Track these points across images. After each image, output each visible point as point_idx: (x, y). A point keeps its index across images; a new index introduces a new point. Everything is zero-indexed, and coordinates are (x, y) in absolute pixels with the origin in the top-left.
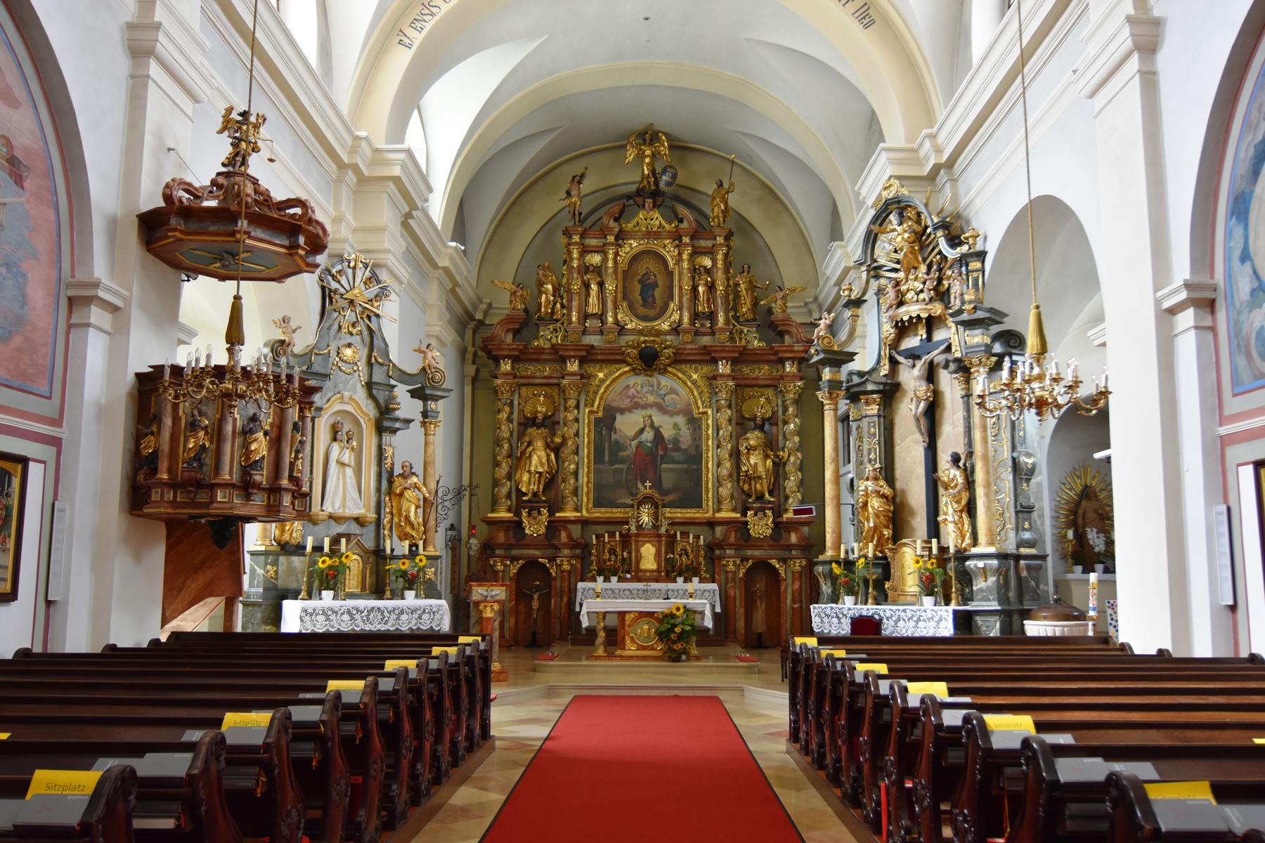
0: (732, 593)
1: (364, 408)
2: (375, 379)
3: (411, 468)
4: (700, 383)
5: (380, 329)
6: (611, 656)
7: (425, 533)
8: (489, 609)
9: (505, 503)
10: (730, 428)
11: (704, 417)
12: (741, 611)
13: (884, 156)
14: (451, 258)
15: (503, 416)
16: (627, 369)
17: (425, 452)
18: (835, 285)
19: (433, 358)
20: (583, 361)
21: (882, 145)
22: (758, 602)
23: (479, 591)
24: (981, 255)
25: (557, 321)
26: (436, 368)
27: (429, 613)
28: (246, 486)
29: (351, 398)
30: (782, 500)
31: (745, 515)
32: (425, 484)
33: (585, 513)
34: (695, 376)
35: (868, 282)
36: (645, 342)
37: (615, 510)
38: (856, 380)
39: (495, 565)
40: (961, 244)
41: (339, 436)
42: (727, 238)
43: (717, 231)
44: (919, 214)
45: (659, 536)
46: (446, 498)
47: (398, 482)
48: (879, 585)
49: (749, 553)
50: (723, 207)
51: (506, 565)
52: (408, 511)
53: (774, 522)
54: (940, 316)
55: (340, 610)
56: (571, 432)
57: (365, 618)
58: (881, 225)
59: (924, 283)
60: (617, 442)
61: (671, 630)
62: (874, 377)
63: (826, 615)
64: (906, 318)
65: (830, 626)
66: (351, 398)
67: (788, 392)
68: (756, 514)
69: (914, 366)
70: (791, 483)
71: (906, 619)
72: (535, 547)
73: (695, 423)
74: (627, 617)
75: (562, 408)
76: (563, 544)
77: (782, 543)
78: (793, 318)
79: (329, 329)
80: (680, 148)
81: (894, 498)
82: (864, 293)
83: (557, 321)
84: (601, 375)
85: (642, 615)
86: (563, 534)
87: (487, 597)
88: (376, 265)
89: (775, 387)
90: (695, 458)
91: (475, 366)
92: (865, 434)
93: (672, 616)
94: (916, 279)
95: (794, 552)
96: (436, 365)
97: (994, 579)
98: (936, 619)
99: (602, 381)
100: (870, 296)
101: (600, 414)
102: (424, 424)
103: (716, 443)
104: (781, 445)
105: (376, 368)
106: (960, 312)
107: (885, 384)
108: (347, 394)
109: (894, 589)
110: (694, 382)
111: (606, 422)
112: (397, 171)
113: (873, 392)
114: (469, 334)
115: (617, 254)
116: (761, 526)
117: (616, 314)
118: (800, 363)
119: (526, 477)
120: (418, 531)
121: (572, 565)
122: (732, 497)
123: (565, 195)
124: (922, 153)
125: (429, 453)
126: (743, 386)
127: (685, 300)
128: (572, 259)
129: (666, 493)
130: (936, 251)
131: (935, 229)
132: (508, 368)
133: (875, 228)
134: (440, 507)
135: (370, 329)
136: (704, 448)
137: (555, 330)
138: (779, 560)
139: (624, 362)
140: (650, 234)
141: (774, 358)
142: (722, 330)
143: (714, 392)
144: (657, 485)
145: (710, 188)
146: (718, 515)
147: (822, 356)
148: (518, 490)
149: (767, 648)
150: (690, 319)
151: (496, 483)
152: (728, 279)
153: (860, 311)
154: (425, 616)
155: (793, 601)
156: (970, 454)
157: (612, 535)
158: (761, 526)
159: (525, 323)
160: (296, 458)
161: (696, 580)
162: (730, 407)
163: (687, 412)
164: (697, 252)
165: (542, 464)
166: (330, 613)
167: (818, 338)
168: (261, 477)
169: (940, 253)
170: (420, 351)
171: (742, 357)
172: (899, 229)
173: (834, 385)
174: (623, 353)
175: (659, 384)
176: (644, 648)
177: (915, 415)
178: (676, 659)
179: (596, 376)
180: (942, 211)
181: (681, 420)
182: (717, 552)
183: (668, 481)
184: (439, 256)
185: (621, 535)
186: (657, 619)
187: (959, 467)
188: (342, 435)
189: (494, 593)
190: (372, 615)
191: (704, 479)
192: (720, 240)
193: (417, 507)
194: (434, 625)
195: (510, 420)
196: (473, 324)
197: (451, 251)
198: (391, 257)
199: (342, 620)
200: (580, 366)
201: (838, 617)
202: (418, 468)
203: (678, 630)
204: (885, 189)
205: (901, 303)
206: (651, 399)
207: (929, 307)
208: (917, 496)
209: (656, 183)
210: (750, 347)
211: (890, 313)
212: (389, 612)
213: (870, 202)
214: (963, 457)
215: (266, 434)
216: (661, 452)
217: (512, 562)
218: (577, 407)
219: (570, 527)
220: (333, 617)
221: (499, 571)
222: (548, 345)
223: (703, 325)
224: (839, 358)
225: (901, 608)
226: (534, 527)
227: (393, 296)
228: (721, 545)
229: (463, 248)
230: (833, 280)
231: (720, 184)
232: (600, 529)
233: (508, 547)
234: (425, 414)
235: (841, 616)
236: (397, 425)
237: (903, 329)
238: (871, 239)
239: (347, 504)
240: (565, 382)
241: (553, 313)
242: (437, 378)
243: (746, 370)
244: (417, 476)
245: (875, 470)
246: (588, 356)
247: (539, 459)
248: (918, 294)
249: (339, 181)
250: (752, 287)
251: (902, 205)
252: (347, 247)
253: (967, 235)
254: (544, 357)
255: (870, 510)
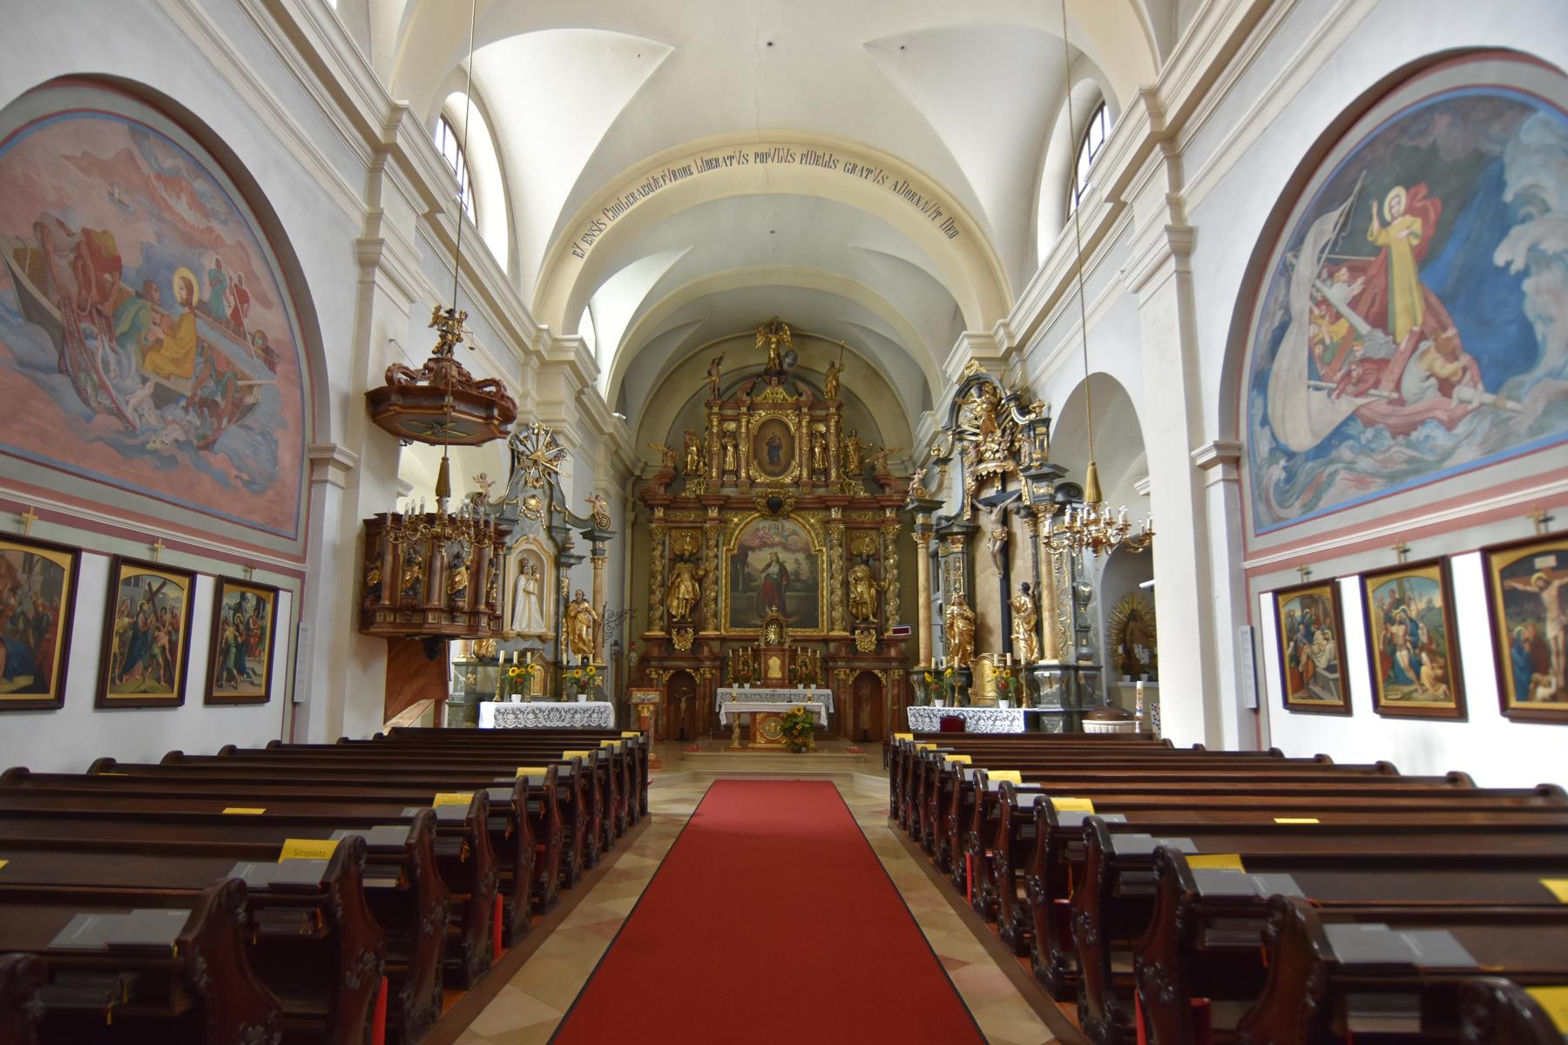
0: (843, 697)
2: (553, 524)
4: (817, 526)
5: (558, 483)
6: (744, 748)
7: (594, 648)
9: (658, 624)
10: (841, 563)
11: (820, 554)
12: (850, 712)
13: (966, 342)
14: (615, 426)
15: (657, 553)
16: (757, 515)
17: (595, 583)
18: (927, 446)
20: (721, 509)
21: (964, 332)
22: (864, 704)
24: (1046, 422)
25: (701, 476)
28: (452, 611)
29: (535, 539)
30: (884, 621)
31: (853, 633)
32: (594, 609)
33: (723, 631)
34: (812, 521)
35: (953, 444)
36: (771, 493)
37: (747, 629)
38: (944, 523)
39: (650, 674)
40: (1029, 412)
41: (525, 571)
42: (839, 408)
43: (830, 403)
44: (995, 388)
45: (784, 650)
47: (573, 607)
48: (963, 691)
49: (857, 664)
50: (834, 383)
51: (659, 674)
52: (581, 630)
53: (877, 639)
54: (1012, 472)
56: (712, 566)
58: (964, 397)
59: (999, 445)
60: (749, 574)
61: (794, 727)
62: (959, 521)
64: (984, 473)
66: (535, 539)
67: (888, 533)
68: (862, 633)
69: (991, 512)
70: (891, 607)
72: (683, 659)
73: (812, 559)
74: (758, 716)
75: (704, 547)
76: (706, 657)
77: (884, 656)
78: (893, 473)
79: (518, 483)
80: (799, 335)
81: (975, 620)
82: (950, 453)
83: (701, 476)
84: (736, 520)
85: (770, 715)
86: (706, 649)
88: (555, 432)
89: (878, 529)
90: (813, 587)
92: (952, 567)
93: (794, 715)
94: (993, 441)
95: (893, 664)
97: (1058, 686)
99: (737, 525)
100: (955, 455)
101: (735, 552)
102: (593, 560)
103: (829, 575)
104: (882, 577)
105: (555, 515)
106: (1029, 468)
107: (967, 527)
108: (531, 536)
109: (976, 694)
110: (812, 526)
111: (740, 559)
112: (572, 356)
113: (958, 533)
114: (629, 487)
115: (748, 422)
116: (866, 643)
117: (748, 473)
118: (898, 510)
119: (675, 603)
120: (588, 646)
121: (713, 674)
122: (843, 619)
123: (706, 374)
124: (997, 339)
126: (852, 529)
127: (804, 459)
128: (712, 426)
129: (790, 615)
130: (1009, 418)
131: (1009, 400)
132: (661, 514)
133: (959, 400)
136: (820, 579)
137: (699, 484)
138: (881, 670)
139: (755, 509)
140: (775, 406)
141: (877, 505)
142: (835, 483)
143: (827, 534)
144: (782, 609)
145: (824, 368)
146: (831, 634)
147: (916, 504)
148: (669, 614)
149: (871, 741)
150: (808, 474)
151: (651, 608)
152: (839, 442)
153: (947, 468)
154: (595, 715)
155: (893, 704)
156: (1038, 584)
157: (745, 649)
158: (866, 643)
159: (675, 478)
160: (492, 588)
161: (813, 686)
162: (841, 545)
163: (806, 550)
164: (814, 420)
165: (688, 592)
167: (913, 489)
168: (463, 603)
169: (1012, 420)
170: (590, 501)
171: (850, 505)
172: (978, 400)
173: (926, 528)
174: (754, 502)
175: (783, 527)
176: (772, 742)
177: (993, 552)
178: (798, 751)
179: (732, 521)
180: (1014, 385)
181: (801, 556)
182: (831, 664)
183: (790, 606)
185: (752, 649)
186: (782, 718)
187: (1028, 595)
188: (528, 569)
189: (650, 697)
191: (820, 604)
192: (832, 410)
193: (588, 627)
195: (662, 556)
197: (615, 420)
200: (719, 512)
202: (589, 596)
203: (799, 727)
204: (967, 368)
205: (980, 461)
206: (777, 539)
207: (1003, 464)
208: (994, 618)
209: (781, 364)
210: (857, 497)
211: (972, 469)
213: (955, 379)
214: (1032, 586)
215: (467, 568)
216: (785, 583)
217: (664, 671)
218: (717, 546)
219: (712, 643)
221: (653, 679)
222: (693, 496)
223: (819, 479)
225: (982, 709)
226: (682, 643)
227: (569, 457)
228: (834, 658)
230: (925, 443)
231: (833, 365)
232: (734, 645)
233: (661, 659)
234: (594, 552)
236: (572, 561)
237: (982, 482)
238: (956, 409)
239: (532, 624)
240: (707, 525)
241: (697, 470)
243: (854, 515)
245: (959, 597)
246: (726, 505)
247: (686, 588)
248: (994, 453)
249: (525, 364)
250: (858, 448)
251: (981, 381)
253: (1035, 405)
254: (690, 505)
255: (956, 629)
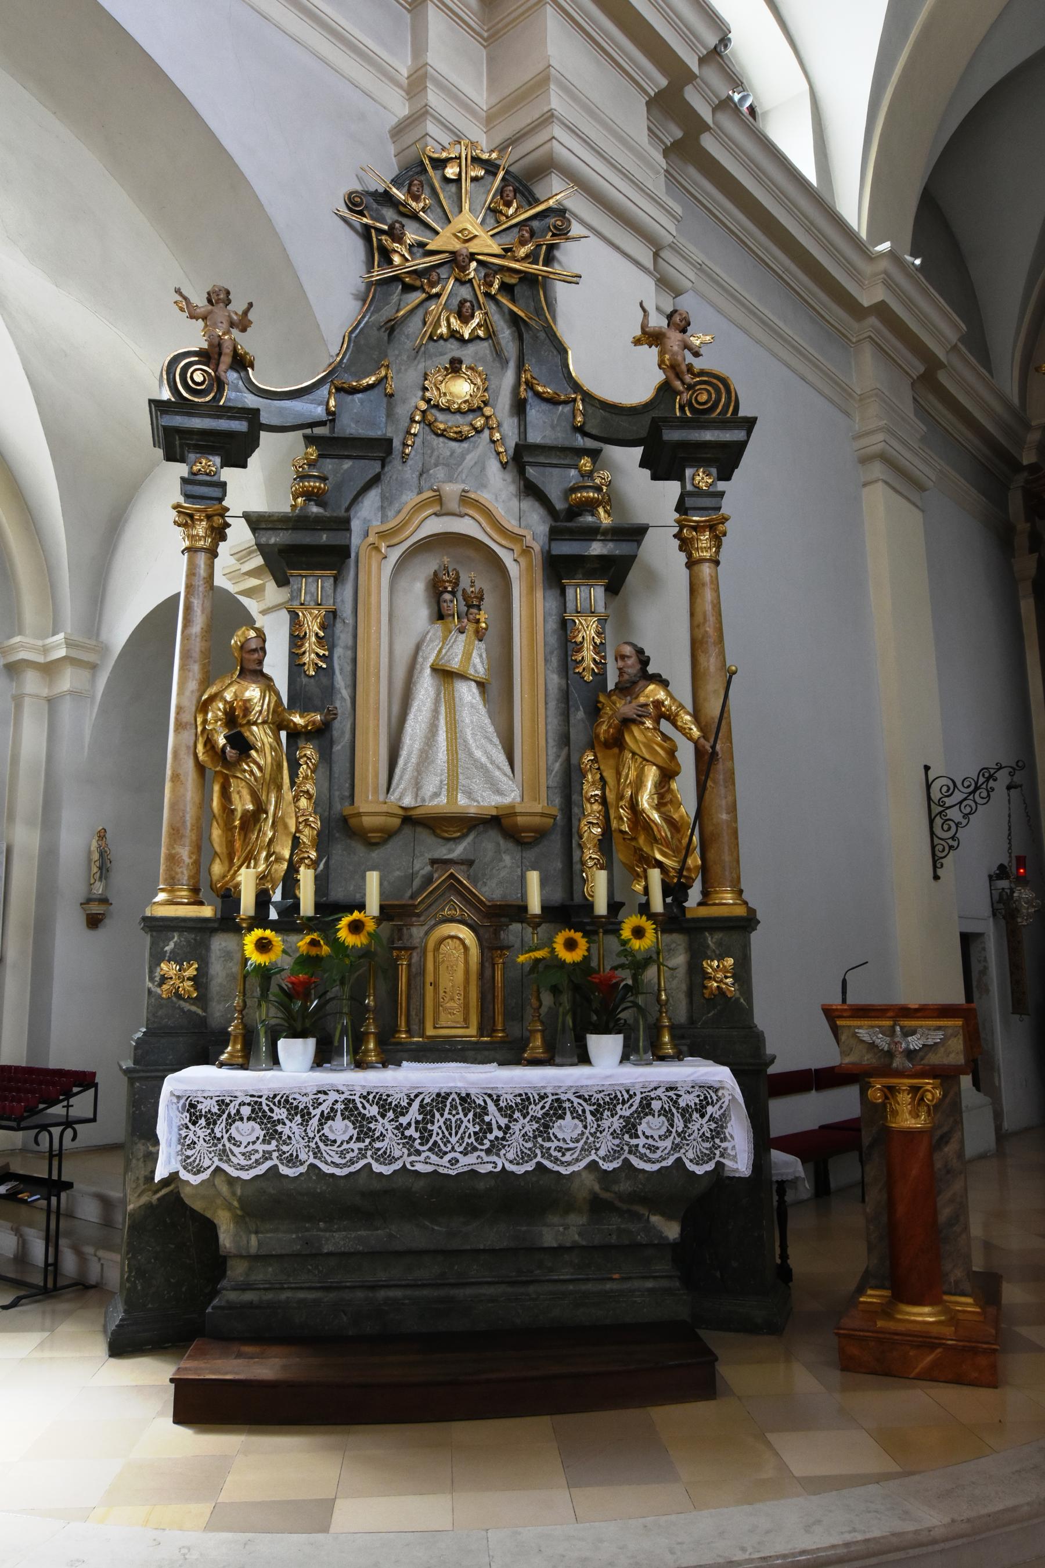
1: (511, 524)
2: (535, 437)
3: (645, 662)
8: (904, 1098)
14: (889, 283)
17: (692, 614)
19: (687, 346)
23: (864, 1034)
26: (702, 373)
27: (664, 1112)
32: (696, 716)
46: (949, 802)
52: (638, 784)
55: (317, 1104)
57: (411, 1132)
66: (465, 499)
87: (890, 1054)
91: (1035, 556)
96: (698, 364)
105: (535, 412)
108: (451, 489)
114: (1016, 502)
125: (699, 618)
134: (938, 821)
135: (515, 321)
154: (652, 1125)
166: (280, 1113)
184: (860, 284)
188: (454, 604)
189: (915, 1042)
190: (439, 1120)
194: (688, 1155)
196: (1021, 479)
197: (884, 264)
198: (557, 131)
199: (325, 1140)
212: (507, 1111)
220: (291, 1128)
229: (918, 262)
239: (462, 780)
242: (704, 397)
244: (664, 683)
252: (431, 128)
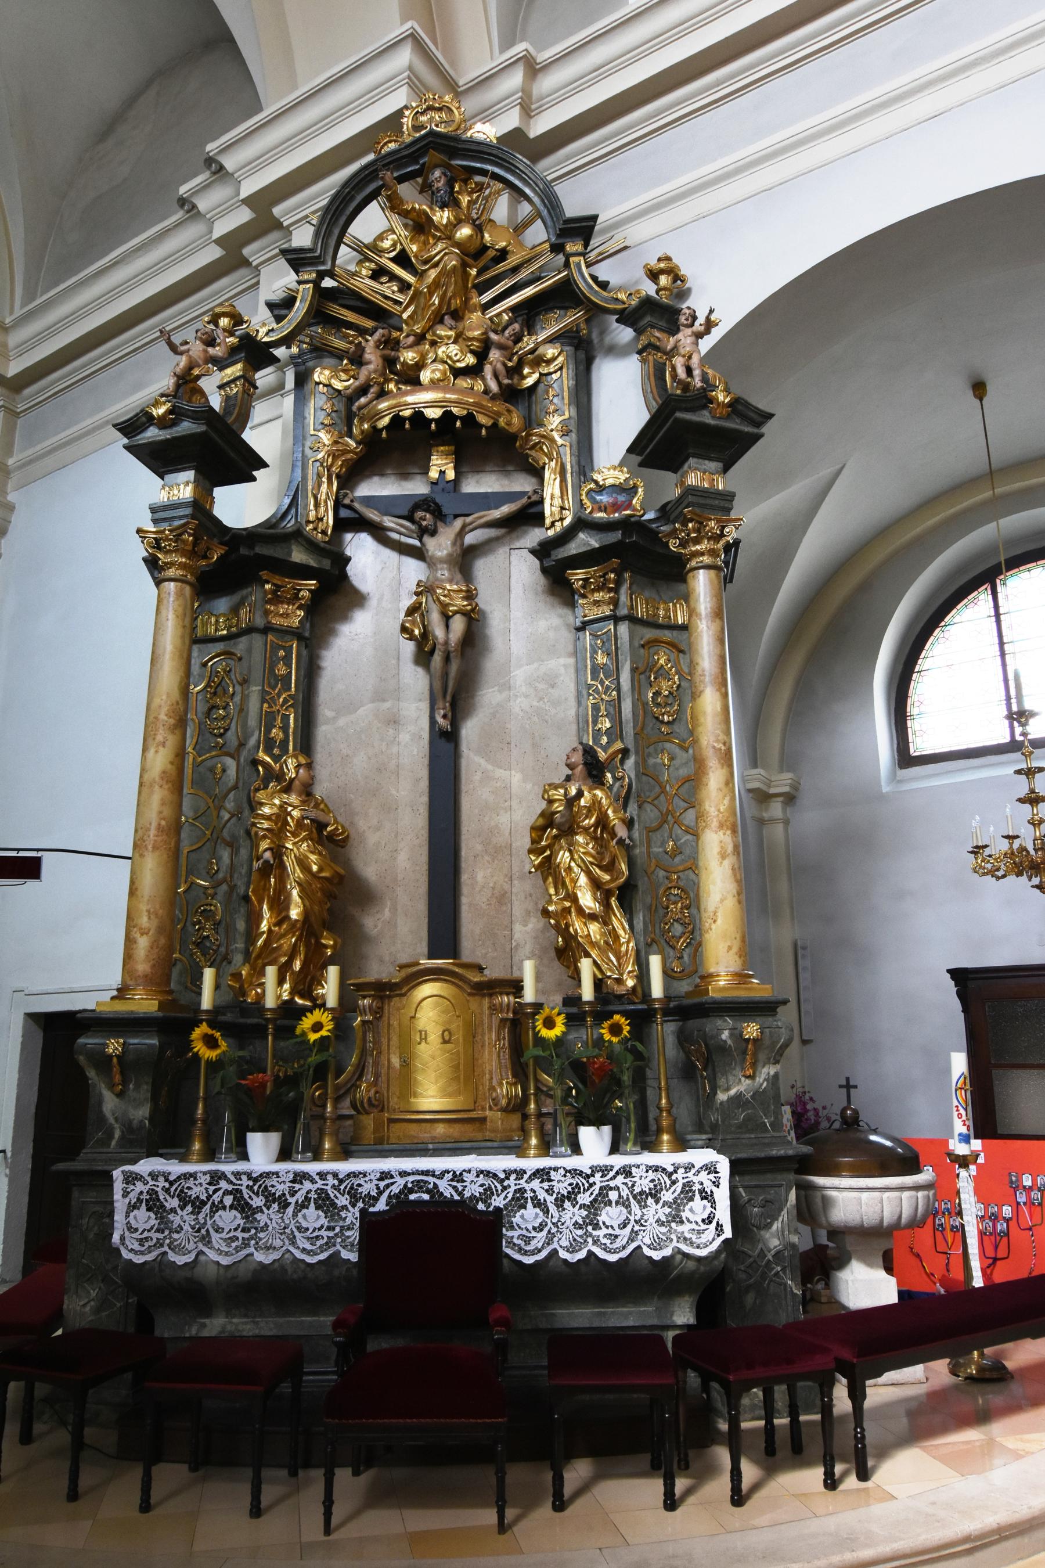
63: (184, 1203)
65: (206, 1240)
71: (550, 1199)
98: (667, 1196)
147: (186, 427)
201: (241, 1205)
224: (232, 454)
235: (258, 1202)
